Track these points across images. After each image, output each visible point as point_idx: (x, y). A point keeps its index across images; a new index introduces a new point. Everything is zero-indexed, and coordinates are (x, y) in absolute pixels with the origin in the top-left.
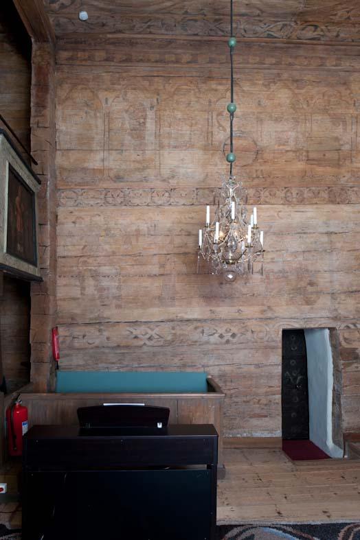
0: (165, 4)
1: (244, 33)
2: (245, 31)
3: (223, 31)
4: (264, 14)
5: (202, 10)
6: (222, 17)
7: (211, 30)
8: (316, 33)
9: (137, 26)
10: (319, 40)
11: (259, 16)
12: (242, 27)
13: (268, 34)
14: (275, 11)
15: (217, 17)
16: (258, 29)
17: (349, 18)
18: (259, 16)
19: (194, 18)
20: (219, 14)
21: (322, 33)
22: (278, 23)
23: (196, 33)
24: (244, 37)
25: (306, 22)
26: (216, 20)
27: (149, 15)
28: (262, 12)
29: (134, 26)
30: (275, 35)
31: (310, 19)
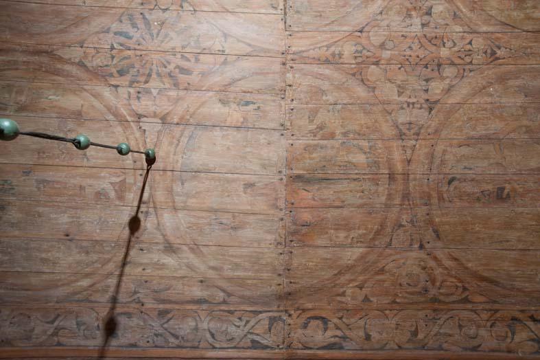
0: (79, 284)
1: (211, 340)
2: (213, 335)
3: (177, 337)
4: (233, 299)
5: (136, 292)
6: (168, 306)
7: (156, 335)
8: (329, 333)
9: (36, 332)
10: (341, 348)
11: (224, 302)
12: (205, 325)
13: (253, 341)
14: (247, 293)
15: (161, 306)
16: (232, 329)
17: (366, 299)
18: (224, 302)
19: (126, 309)
20: (164, 301)
21: (339, 333)
22: (261, 316)
23: (132, 342)
24: (214, 348)
25: (304, 310)
26: (162, 313)
27: (57, 306)
28: (229, 295)
29: (33, 330)
30: (264, 342)
31: (309, 305)
